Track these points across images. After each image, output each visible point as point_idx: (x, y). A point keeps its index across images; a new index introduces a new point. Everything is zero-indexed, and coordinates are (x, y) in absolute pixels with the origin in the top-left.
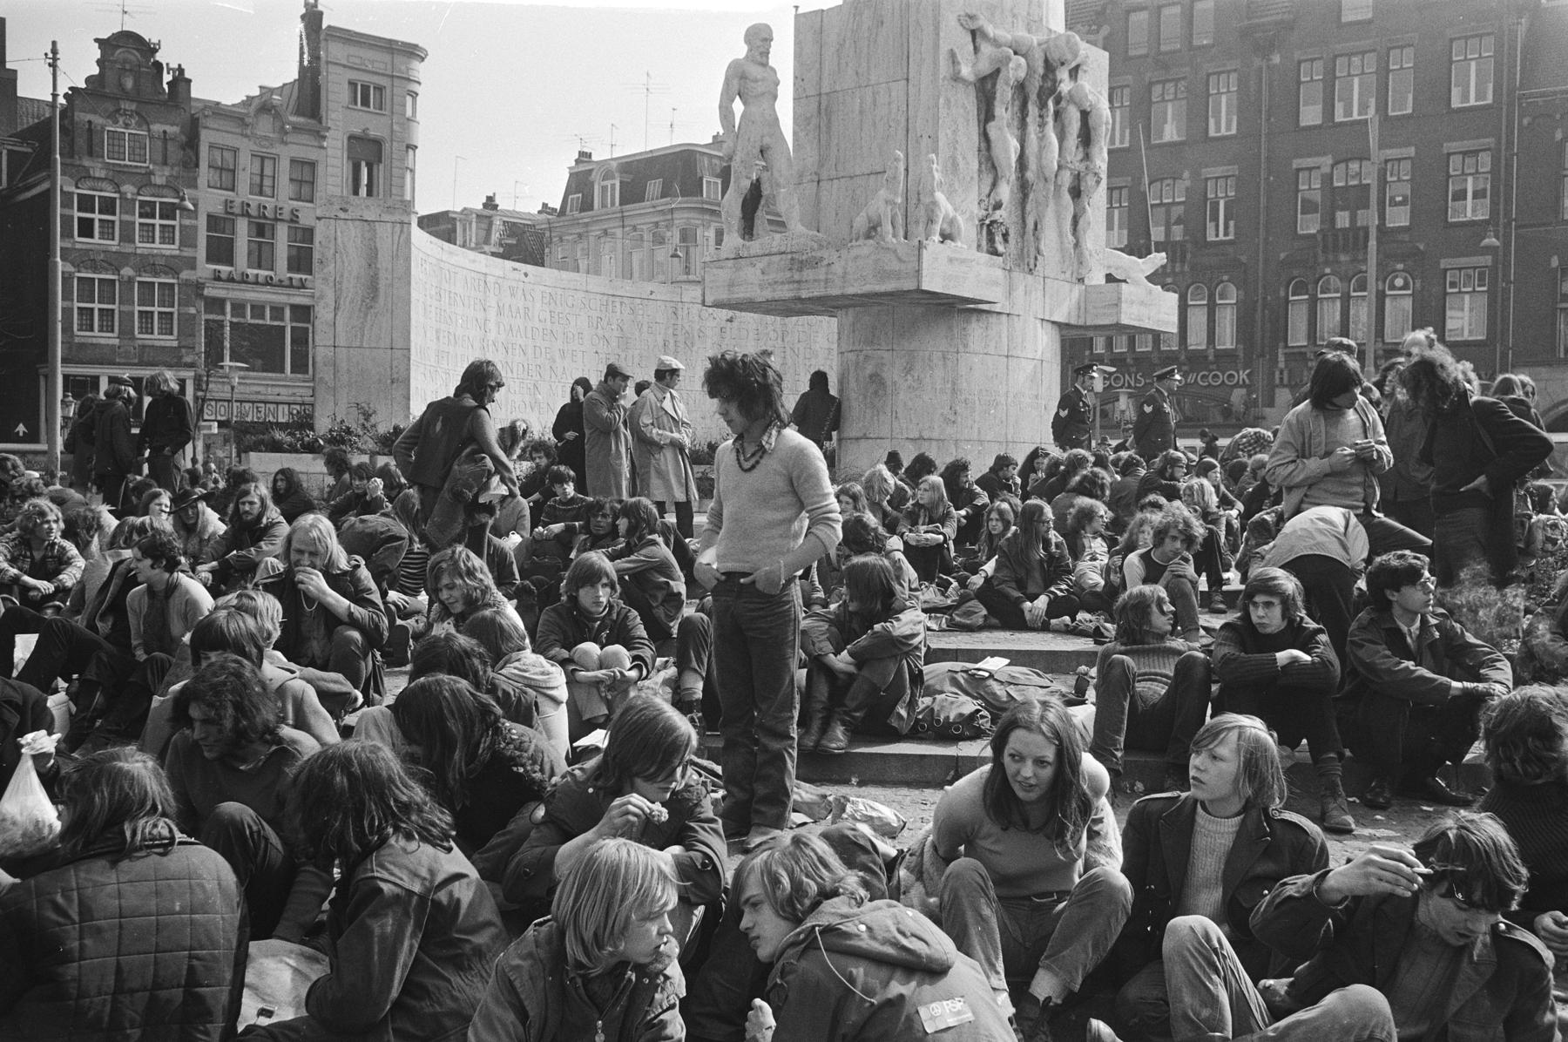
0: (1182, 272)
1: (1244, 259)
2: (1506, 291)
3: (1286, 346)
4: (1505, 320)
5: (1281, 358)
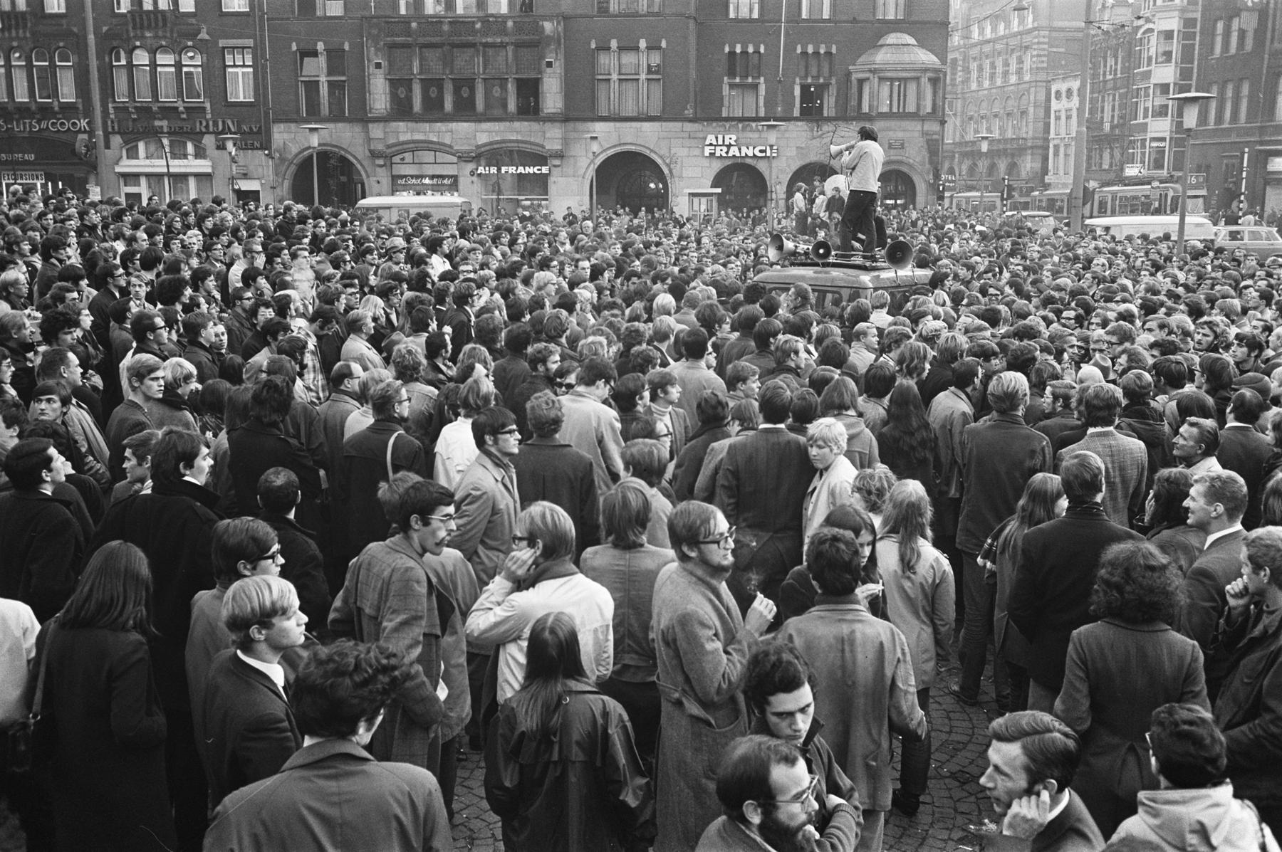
0: (25, 38)
1: (75, 30)
2: (264, 67)
3: (114, 102)
4: (265, 88)
5: (111, 111)
